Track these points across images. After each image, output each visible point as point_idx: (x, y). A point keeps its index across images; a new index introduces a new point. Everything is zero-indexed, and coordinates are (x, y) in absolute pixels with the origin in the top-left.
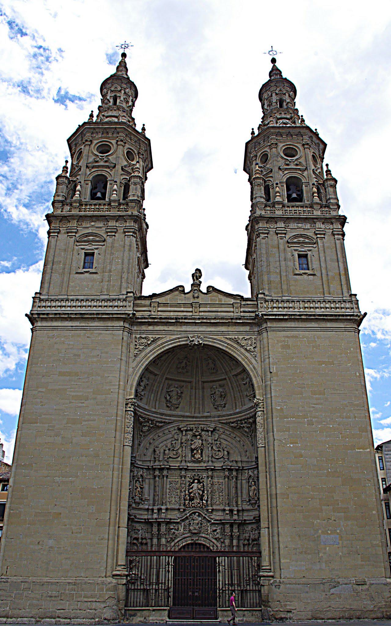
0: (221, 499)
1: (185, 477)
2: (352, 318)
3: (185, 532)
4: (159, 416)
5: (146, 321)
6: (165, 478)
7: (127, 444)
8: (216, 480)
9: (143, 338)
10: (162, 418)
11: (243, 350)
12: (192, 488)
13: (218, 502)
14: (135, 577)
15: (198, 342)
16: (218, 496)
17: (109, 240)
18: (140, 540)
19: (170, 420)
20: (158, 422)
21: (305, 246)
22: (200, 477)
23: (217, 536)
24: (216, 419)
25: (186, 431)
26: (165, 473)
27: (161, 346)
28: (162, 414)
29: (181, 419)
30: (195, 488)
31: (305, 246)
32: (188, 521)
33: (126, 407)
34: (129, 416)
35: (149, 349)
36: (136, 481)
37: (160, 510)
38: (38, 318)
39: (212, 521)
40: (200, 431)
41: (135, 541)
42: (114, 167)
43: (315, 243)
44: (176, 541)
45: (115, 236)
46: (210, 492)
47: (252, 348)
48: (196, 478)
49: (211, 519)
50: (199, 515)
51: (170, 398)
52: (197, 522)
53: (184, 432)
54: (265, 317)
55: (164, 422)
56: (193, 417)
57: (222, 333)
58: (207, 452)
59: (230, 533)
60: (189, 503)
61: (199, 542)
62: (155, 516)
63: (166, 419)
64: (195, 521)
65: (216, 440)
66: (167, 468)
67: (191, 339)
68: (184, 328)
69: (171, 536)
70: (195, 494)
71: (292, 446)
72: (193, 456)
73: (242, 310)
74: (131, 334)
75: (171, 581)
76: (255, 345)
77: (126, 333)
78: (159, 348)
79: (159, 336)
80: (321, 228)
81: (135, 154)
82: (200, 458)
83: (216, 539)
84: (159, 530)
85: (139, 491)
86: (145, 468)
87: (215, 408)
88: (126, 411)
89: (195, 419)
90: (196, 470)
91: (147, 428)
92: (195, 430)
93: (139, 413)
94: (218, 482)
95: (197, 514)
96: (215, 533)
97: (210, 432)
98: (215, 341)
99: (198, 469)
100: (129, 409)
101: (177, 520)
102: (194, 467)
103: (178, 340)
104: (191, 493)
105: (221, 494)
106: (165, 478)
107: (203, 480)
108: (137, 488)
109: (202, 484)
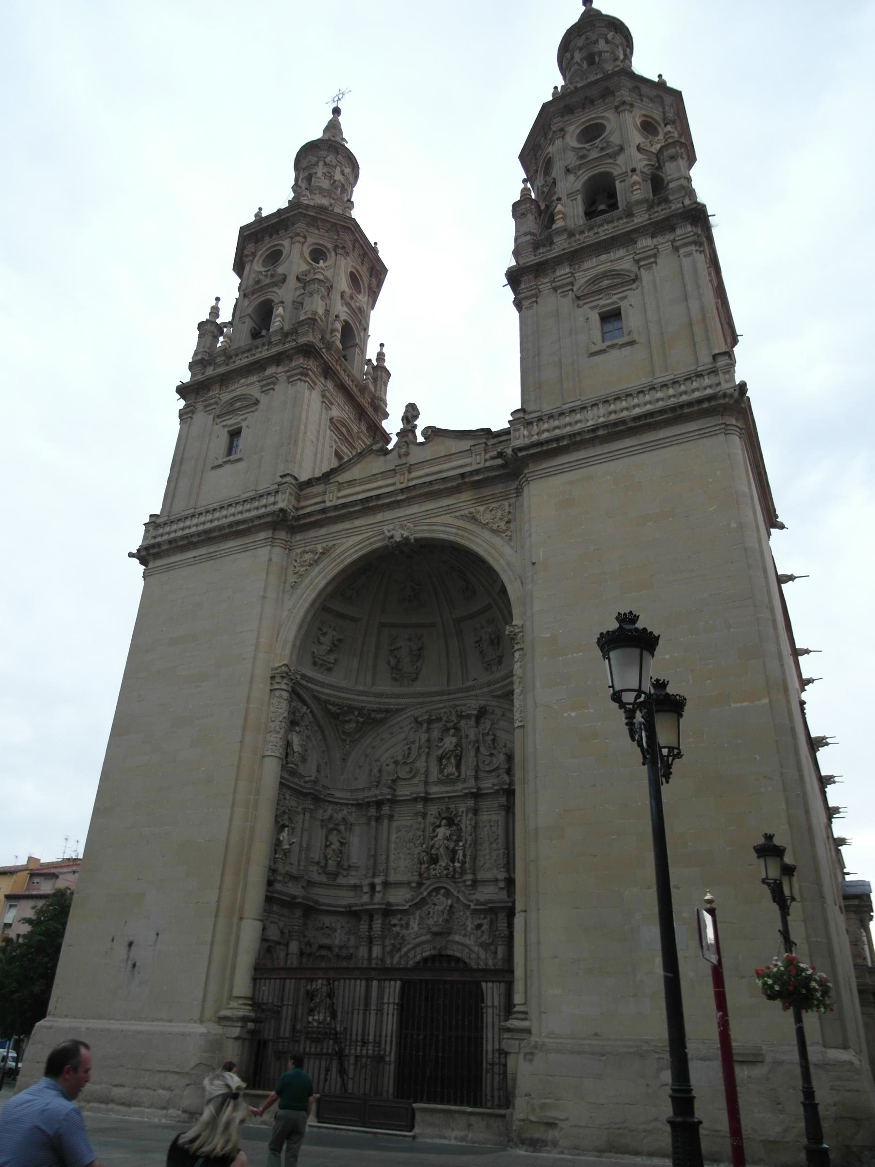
0: (495, 857)
1: (424, 815)
2: (713, 403)
3: (421, 931)
4: (372, 699)
5: (313, 519)
6: (386, 822)
7: (269, 753)
8: (484, 817)
9: (307, 553)
10: (380, 703)
11: (487, 534)
12: (436, 836)
13: (488, 865)
14: (318, 1027)
15: (402, 535)
16: (487, 851)
17: (264, 399)
18: (336, 950)
19: (398, 704)
20: (374, 711)
21: (614, 292)
22: (452, 812)
23: (483, 939)
24: (486, 690)
25: (430, 722)
26: (386, 810)
27: (338, 561)
28: (380, 695)
29: (420, 700)
30: (440, 836)
31: (614, 292)
32: (426, 908)
33: (272, 684)
34: (276, 699)
35: (317, 569)
36: (332, 830)
37: (373, 886)
38: (148, 554)
39: (473, 907)
40: (454, 718)
41: (324, 952)
42: (284, 280)
43: (634, 281)
44: (404, 950)
45: (273, 389)
46: (469, 842)
47: (502, 524)
48: (444, 815)
49: (471, 901)
50: (448, 894)
51: (398, 662)
52: (441, 908)
53: (425, 725)
54: (520, 454)
55: (387, 711)
56: (442, 693)
57: (448, 510)
58: (469, 759)
59: (506, 932)
60: (428, 869)
61: (450, 952)
62: (366, 898)
63: (390, 704)
64: (437, 908)
65: (488, 734)
66: (388, 799)
67: (388, 534)
68: (380, 517)
69: (392, 942)
70: (438, 849)
71: (573, 714)
72: (441, 771)
73: (488, 456)
74: (290, 550)
75: (392, 1037)
76: (511, 516)
77: (277, 550)
78: (334, 564)
79: (333, 543)
80: (647, 246)
81: (328, 250)
82: (453, 774)
83: (481, 945)
84: (370, 927)
85: (334, 850)
86: (352, 805)
87: (487, 670)
88: (271, 690)
89: (446, 697)
90: (447, 800)
91: (353, 725)
92: (444, 719)
93: (323, 697)
94: (490, 821)
95: (442, 891)
96: (479, 933)
97: (473, 719)
98: (434, 527)
99: (449, 797)
100: (277, 686)
101: (404, 905)
102: (442, 793)
103: (367, 542)
104: (432, 847)
105: (494, 846)
106: (386, 822)
107: (458, 819)
108: (331, 843)
109: (454, 828)
